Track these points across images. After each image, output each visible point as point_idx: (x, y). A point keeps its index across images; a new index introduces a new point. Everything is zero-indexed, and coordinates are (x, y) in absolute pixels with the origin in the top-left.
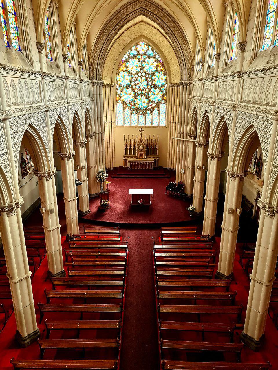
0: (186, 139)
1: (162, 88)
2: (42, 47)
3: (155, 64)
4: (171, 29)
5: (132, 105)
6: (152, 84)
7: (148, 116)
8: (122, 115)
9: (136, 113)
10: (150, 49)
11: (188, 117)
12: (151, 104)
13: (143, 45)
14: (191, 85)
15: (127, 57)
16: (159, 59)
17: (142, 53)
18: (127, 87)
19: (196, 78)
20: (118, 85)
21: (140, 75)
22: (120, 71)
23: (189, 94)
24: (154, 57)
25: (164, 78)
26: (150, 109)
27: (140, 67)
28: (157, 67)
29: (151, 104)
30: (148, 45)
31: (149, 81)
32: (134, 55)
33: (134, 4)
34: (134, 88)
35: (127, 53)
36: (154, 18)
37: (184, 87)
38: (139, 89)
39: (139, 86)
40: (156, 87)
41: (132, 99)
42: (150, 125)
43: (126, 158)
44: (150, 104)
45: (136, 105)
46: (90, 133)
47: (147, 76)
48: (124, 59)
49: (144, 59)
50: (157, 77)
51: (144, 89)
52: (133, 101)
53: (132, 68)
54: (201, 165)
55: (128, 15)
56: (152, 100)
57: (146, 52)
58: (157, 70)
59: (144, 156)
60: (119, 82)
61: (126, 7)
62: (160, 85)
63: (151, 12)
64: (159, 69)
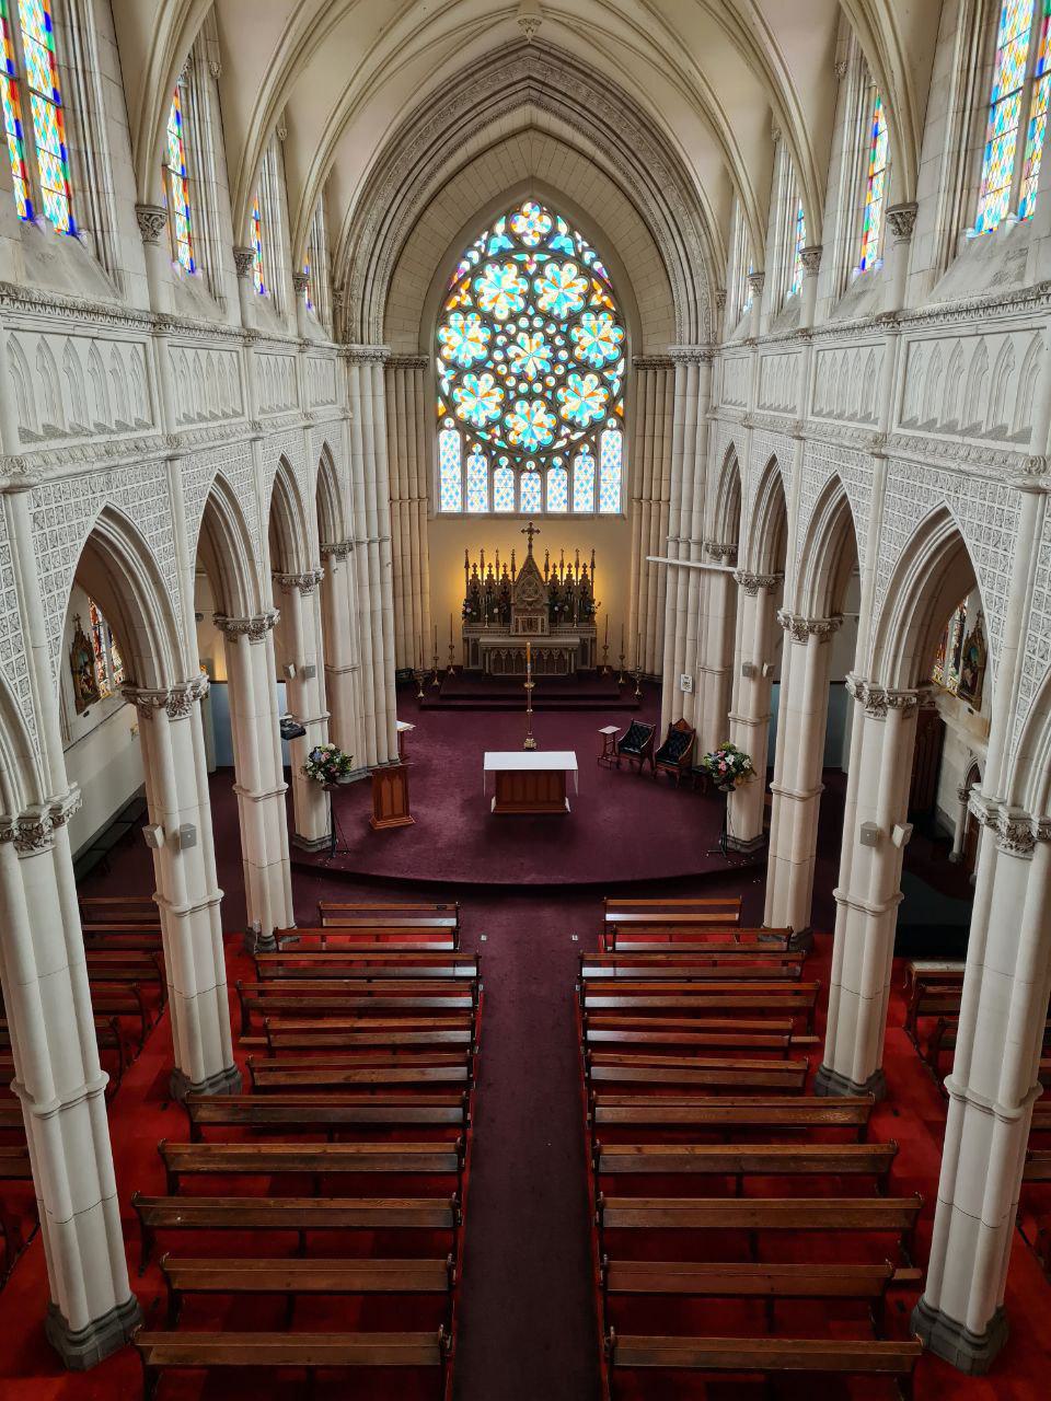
0: (699, 560)
1: (606, 374)
2: (157, 219)
3: (582, 284)
4: (639, 155)
5: (494, 436)
6: (571, 358)
7: (556, 477)
8: (458, 470)
9: (510, 466)
10: (563, 227)
11: (703, 482)
12: (565, 431)
13: (535, 214)
14: (716, 361)
15: (475, 256)
16: (597, 266)
17: (532, 241)
18: (478, 368)
19: (735, 336)
20: (443, 359)
21: (523, 323)
22: (448, 309)
23: (708, 396)
24: (578, 259)
25: (617, 334)
26: (560, 452)
27: (522, 295)
28: (587, 296)
29: (565, 431)
30: (553, 214)
31: (560, 348)
32: (502, 250)
33: (498, 64)
34: (504, 373)
35: (477, 244)
36: (575, 116)
37: (691, 369)
38: (521, 378)
39: (522, 366)
40: (584, 368)
41: (495, 413)
42: (563, 509)
43: (471, 636)
44: (563, 433)
45: (512, 437)
46: (339, 541)
47: (552, 330)
48: (465, 266)
49: (541, 265)
50: (590, 330)
51: (541, 377)
52: (500, 422)
53: (495, 300)
54: (755, 661)
55: (479, 104)
56: (570, 417)
58: (588, 308)
59: (543, 626)
60: (446, 352)
61: (472, 74)
62: (599, 364)
63: (565, 94)
64: (595, 301)
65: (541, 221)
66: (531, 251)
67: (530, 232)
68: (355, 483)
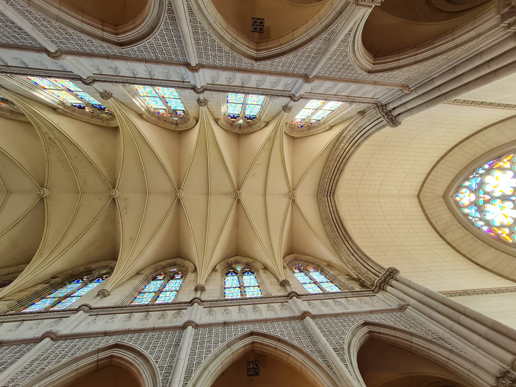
10: (467, 183)
14: (383, 102)
15: (481, 223)
37: (395, 113)
57: (472, 191)
65: (464, 193)
66: (478, 197)
67: (469, 198)
68: (451, 330)
